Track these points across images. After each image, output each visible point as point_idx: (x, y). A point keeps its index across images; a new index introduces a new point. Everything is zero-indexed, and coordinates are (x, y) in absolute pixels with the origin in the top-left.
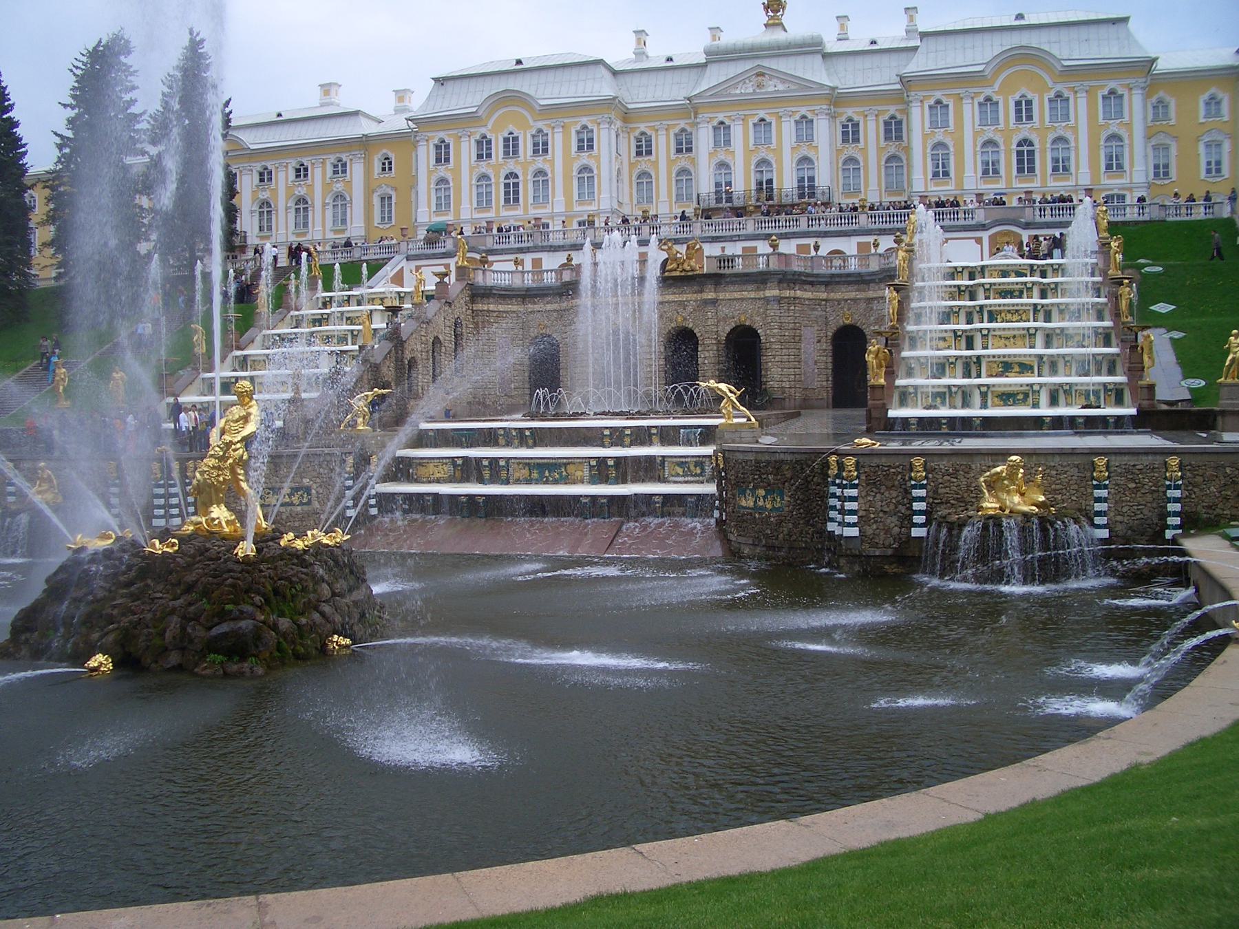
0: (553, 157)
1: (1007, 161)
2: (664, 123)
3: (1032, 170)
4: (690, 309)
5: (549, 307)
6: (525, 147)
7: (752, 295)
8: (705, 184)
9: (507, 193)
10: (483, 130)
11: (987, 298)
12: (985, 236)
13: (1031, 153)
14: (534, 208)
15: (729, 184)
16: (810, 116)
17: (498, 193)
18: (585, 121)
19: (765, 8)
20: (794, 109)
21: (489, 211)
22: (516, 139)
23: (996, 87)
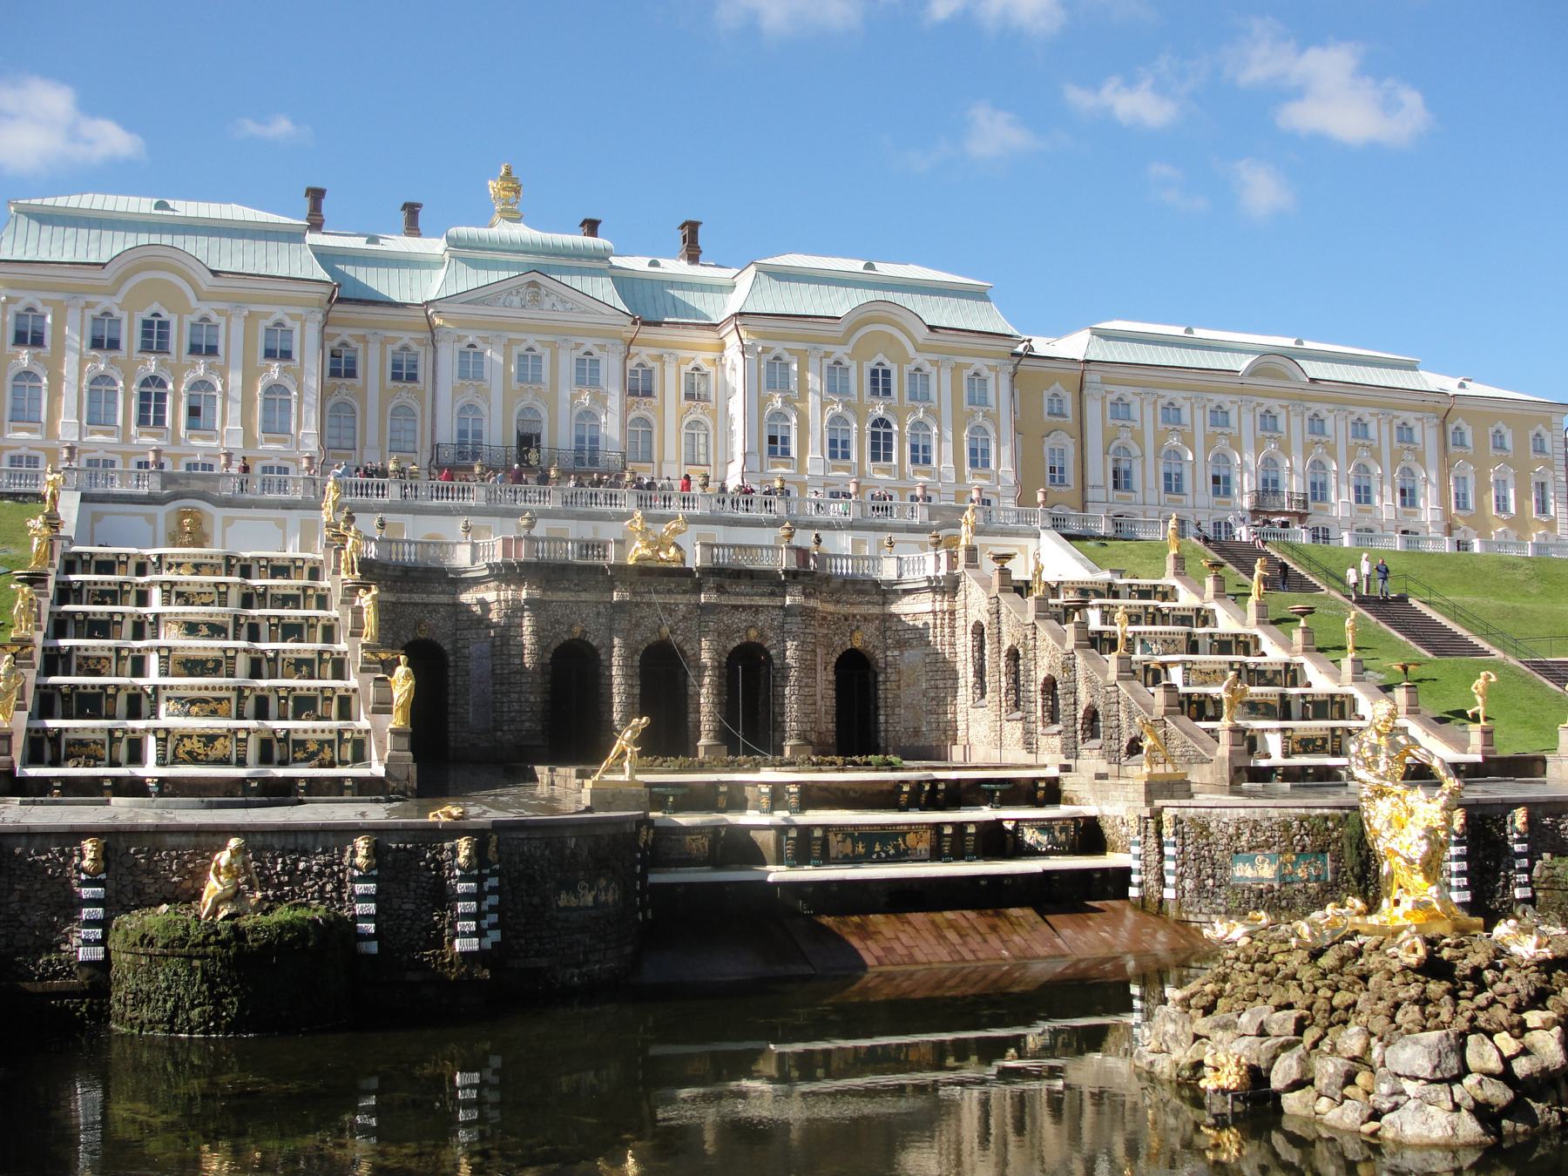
1: (860, 447)
2: (380, 332)
4: (680, 614)
5: (435, 599)
6: (178, 339)
7: (764, 601)
8: (447, 433)
10: (106, 303)
13: (888, 436)
15: (478, 434)
16: (597, 353)
17: (125, 408)
20: (579, 340)
22: (164, 325)
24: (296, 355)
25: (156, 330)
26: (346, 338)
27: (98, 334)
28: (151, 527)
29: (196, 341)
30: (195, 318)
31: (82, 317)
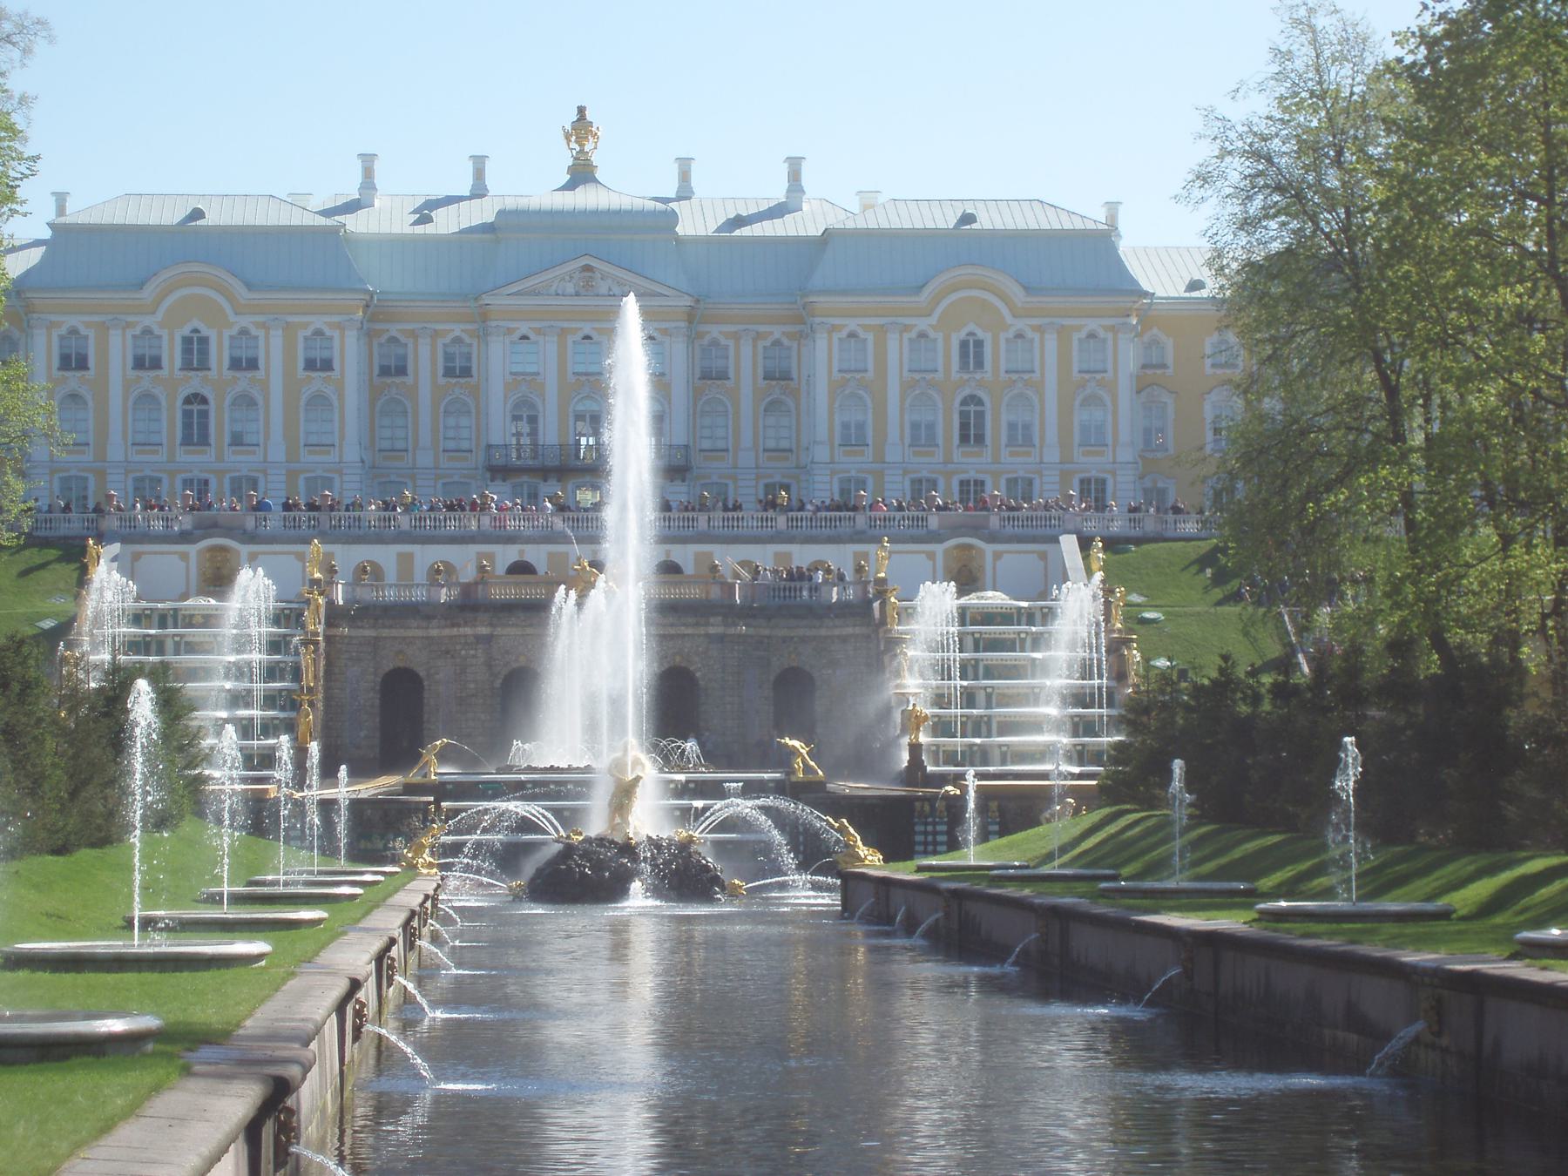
0: (268, 375)
1: (947, 426)
3: (980, 439)
5: (410, 633)
6: (219, 355)
7: (689, 631)
9: (187, 426)
10: (148, 321)
11: (976, 650)
12: (939, 549)
13: (980, 415)
14: (234, 453)
17: (170, 421)
18: (318, 322)
19: (568, 137)
21: (156, 452)
22: (204, 341)
23: (933, 320)
24: (336, 365)
25: (195, 346)
26: (394, 333)
27: (140, 352)
28: (183, 564)
29: (238, 353)
30: (234, 331)
31: (124, 335)
